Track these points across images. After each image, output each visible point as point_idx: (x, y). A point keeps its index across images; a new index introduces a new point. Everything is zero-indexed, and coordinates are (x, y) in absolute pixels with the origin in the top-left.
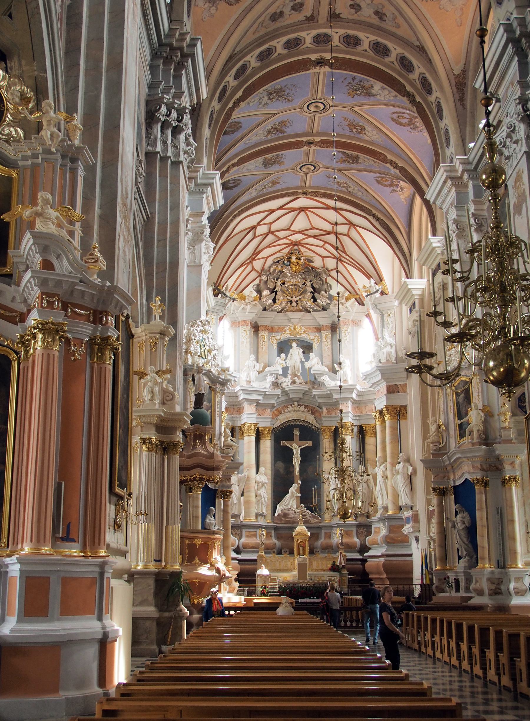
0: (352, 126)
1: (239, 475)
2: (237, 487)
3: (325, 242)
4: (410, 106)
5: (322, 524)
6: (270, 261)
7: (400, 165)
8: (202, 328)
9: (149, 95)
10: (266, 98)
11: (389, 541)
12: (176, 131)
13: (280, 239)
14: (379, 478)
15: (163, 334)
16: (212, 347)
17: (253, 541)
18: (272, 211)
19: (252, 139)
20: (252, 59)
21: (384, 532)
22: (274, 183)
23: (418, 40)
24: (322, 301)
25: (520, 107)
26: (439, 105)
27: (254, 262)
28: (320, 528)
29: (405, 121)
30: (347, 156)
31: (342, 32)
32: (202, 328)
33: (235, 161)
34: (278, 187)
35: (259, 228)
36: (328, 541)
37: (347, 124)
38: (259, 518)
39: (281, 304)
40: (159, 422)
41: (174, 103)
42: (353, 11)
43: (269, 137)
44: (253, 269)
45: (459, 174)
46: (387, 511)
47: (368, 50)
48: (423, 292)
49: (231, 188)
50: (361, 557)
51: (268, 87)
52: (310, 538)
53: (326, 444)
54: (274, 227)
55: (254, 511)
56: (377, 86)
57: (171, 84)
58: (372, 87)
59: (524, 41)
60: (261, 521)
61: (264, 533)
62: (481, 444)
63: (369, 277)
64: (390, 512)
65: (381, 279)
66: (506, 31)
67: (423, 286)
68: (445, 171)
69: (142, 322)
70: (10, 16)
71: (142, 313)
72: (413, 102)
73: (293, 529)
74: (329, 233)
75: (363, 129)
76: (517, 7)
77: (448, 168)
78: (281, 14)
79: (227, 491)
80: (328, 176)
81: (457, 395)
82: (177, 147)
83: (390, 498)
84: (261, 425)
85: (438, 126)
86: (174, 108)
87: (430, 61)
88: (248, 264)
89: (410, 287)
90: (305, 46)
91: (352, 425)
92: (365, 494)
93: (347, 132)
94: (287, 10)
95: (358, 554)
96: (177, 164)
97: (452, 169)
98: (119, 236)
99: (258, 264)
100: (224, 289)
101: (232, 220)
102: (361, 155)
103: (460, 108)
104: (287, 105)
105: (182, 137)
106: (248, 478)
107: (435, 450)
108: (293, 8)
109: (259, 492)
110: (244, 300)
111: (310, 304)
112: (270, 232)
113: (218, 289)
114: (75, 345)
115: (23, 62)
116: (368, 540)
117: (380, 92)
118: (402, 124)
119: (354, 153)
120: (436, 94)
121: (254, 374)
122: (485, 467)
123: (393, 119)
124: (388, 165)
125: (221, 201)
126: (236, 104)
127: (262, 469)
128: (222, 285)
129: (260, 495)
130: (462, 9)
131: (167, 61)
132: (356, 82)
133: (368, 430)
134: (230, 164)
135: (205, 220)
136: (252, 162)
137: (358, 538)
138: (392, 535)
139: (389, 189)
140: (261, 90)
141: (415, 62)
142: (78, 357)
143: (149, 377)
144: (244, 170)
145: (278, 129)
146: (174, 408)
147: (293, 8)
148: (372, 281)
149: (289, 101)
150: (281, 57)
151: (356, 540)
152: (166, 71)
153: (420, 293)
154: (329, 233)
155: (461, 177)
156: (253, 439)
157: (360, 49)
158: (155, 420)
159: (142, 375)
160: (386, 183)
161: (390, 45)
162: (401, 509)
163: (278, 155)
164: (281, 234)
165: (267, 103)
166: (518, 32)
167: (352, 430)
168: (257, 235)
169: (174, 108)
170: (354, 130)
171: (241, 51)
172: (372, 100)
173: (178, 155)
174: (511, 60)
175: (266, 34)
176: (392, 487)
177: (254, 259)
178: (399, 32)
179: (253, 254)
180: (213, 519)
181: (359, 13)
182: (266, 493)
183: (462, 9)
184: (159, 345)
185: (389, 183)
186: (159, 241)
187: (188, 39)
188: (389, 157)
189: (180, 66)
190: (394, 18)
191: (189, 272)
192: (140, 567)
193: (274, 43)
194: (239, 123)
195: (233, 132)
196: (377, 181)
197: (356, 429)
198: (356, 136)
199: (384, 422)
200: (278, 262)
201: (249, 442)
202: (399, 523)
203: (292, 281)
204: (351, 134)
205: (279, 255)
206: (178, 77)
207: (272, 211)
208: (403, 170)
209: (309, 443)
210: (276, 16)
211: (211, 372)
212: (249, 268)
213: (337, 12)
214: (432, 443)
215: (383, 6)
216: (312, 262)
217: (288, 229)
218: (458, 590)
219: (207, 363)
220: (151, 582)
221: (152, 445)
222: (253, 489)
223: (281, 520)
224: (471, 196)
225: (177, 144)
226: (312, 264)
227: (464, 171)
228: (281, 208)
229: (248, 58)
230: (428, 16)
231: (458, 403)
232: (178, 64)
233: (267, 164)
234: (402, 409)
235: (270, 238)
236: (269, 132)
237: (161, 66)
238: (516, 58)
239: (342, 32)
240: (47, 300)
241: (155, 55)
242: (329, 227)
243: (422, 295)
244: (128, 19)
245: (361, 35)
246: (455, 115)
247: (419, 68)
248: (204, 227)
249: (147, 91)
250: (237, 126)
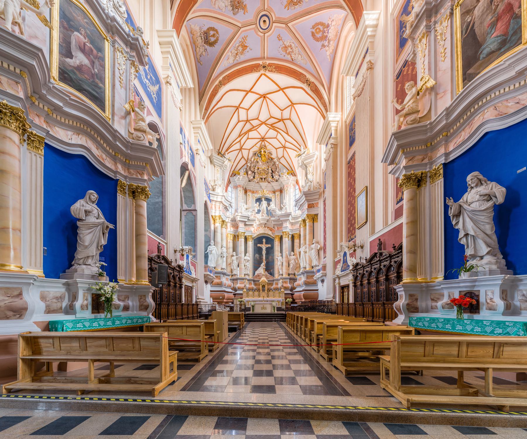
24: (276, 177)
36: (276, 286)
38: (246, 276)
39: (257, 179)
55: (244, 272)
60: (247, 277)
106: (241, 258)
109: (246, 264)
111: (270, 179)
121: (244, 209)
127: (247, 254)
133: (296, 235)
156: (243, 240)
179: (240, 136)
182: (250, 265)
203: (262, 166)
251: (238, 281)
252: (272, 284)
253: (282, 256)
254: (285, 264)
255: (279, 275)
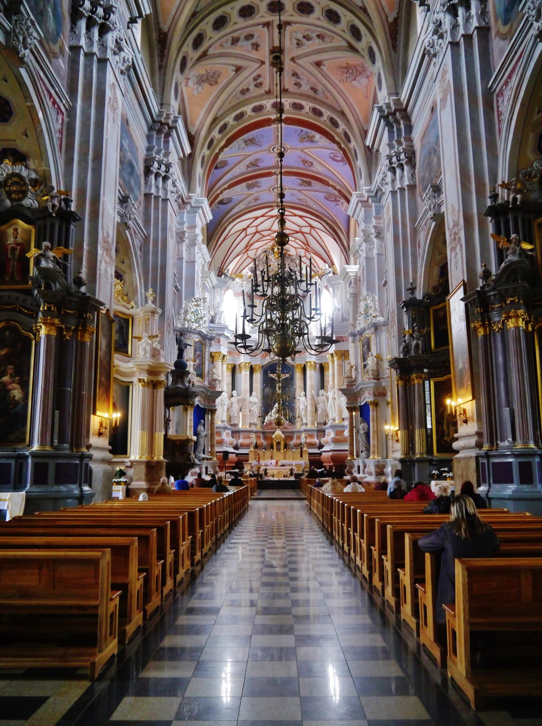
0: (304, 162)
1: (239, 397)
2: (237, 406)
3: (296, 239)
4: (339, 150)
5: (295, 430)
6: (260, 251)
7: (338, 188)
8: (195, 303)
9: (147, 155)
10: (243, 145)
11: (335, 441)
12: (165, 179)
13: (264, 236)
14: (330, 399)
15: (153, 312)
16: (203, 315)
17: (247, 441)
18: (257, 218)
19: (237, 171)
20: (230, 119)
21: (332, 435)
22: (256, 199)
23: (340, 106)
25: (388, 161)
26: (355, 150)
27: (248, 252)
28: (293, 432)
29: (339, 159)
30: (304, 181)
31: (291, 101)
32: (195, 303)
33: (226, 186)
34: (258, 202)
35: (248, 229)
37: (301, 160)
38: (252, 426)
40: (149, 368)
41: (163, 160)
42: (296, 87)
43: (249, 169)
44: (248, 257)
45: (366, 199)
46: (335, 421)
47: (309, 112)
48: (357, 273)
49: (226, 204)
50: (319, 452)
51: (246, 136)
52: (284, 439)
53: (298, 376)
54: (260, 228)
55: (248, 421)
56: (318, 136)
57: (162, 147)
58: (314, 136)
59: (390, 117)
60: (253, 428)
61: (253, 436)
62: (374, 379)
63: (325, 262)
64: (337, 422)
65: (333, 264)
66: (379, 111)
67: (357, 270)
68: (357, 197)
69: (142, 305)
70: (27, 136)
71: (141, 299)
72: (340, 147)
73: (274, 433)
74: (297, 232)
75: (312, 164)
76: (388, 94)
77: (359, 195)
78: (248, 90)
79: (213, 410)
80: (293, 195)
81: (363, 346)
82: (165, 189)
83: (337, 412)
84: (253, 363)
85: (355, 165)
86: (163, 164)
87: (347, 121)
88: (244, 253)
89: (347, 270)
90: (267, 110)
91: (315, 363)
92: (323, 410)
93: (301, 165)
94: (252, 87)
95: (317, 450)
96: (165, 200)
97: (361, 196)
98: (101, 262)
99: (251, 253)
100: (226, 271)
101: (228, 225)
102: (313, 182)
103: (368, 153)
104: (259, 149)
105: (170, 182)
107: (349, 382)
108: (256, 86)
109: (252, 409)
110: (242, 278)
112: (257, 232)
113: (222, 272)
114: (66, 331)
115: (36, 161)
116: (323, 440)
117: (320, 140)
118: (337, 161)
119: (308, 180)
120: (353, 144)
122: (376, 393)
123: (331, 158)
124: (330, 188)
125: (210, 217)
126: (221, 150)
127: (254, 393)
128: (224, 268)
129: (253, 411)
130: (367, 87)
131: (159, 132)
132: (303, 133)
134: (222, 188)
135: (198, 231)
136: (239, 186)
137: (318, 438)
138: (337, 437)
139: (334, 203)
140: (239, 140)
141: (339, 122)
142: (68, 338)
143: (143, 340)
144: (234, 191)
145: (254, 164)
146: (159, 359)
147: (256, 86)
148: (327, 266)
149: (259, 146)
150: (250, 117)
151: (316, 440)
152: (158, 139)
153: (355, 274)
154: (297, 232)
155: (367, 201)
156: (248, 373)
157: (303, 111)
158: (146, 368)
159: (139, 339)
160: (332, 199)
161: (323, 110)
162: (344, 419)
163: (256, 182)
164: (264, 233)
165: (244, 148)
166: (386, 112)
167: (315, 366)
168: (248, 234)
169: (163, 164)
170: (306, 165)
171: (222, 115)
172: (315, 145)
173: (167, 194)
174: (384, 129)
175: (239, 103)
176: (338, 405)
177: (247, 250)
178: (328, 101)
179: (246, 247)
180: (202, 428)
181: (301, 88)
182: (257, 409)
183: (367, 87)
184: (150, 320)
185: (333, 199)
186: (153, 251)
187: (172, 117)
188: (331, 183)
189: (168, 135)
190: (324, 93)
191: (187, 266)
192: (137, 458)
193: (244, 109)
194: (226, 161)
195: (222, 167)
196: (325, 198)
197: (318, 366)
198: (308, 168)
199: (333, 362)
200: (265, 251)
201: (246, 375)
202: (342, 429)
204: (304, 167)
205: (265, 247)
206: (166, 142)
207: (257, 218)
208: (340, 192)
209: (287, 376)
210: (243, 92)
211: (202, 332)
212: (245, 256)
213: (286, 87)
214: (347, 378)
215: (316, 85)
216: (288, 251)
217: (270, 230)
218: (359, 473)
219: (199, 326)
220: (143, 467)
221: (145, 383)
222: (247, 407)
223: (268, 427)
224: (374, 214)
225: (166, 187)
226: (289, 253)
227: (368, 197)
228: (263, 216)
229: (227, 119)
230: (345, 91)
231: (363, 352)
232: (167, 133)
233: (249, 187)
234: (346, 353)
235: (258, 236)
236: (248, 167)
237: (155, 135)
238: (387, 128)
239: (291, 101)
240: (48, 307)
241: (150, 129)
242: (297, 229)
243: (356, 276)
244: (107, 126)
245: (303, 103)
246: (365, 157)
247: (342, 126)
248: (196, 235)
249: (145, 152)
250: (224, 163)
251: (241, 435)
252: (291, 438)
253: (305, 396)
254: (309, 408)
255: (303, 424)
